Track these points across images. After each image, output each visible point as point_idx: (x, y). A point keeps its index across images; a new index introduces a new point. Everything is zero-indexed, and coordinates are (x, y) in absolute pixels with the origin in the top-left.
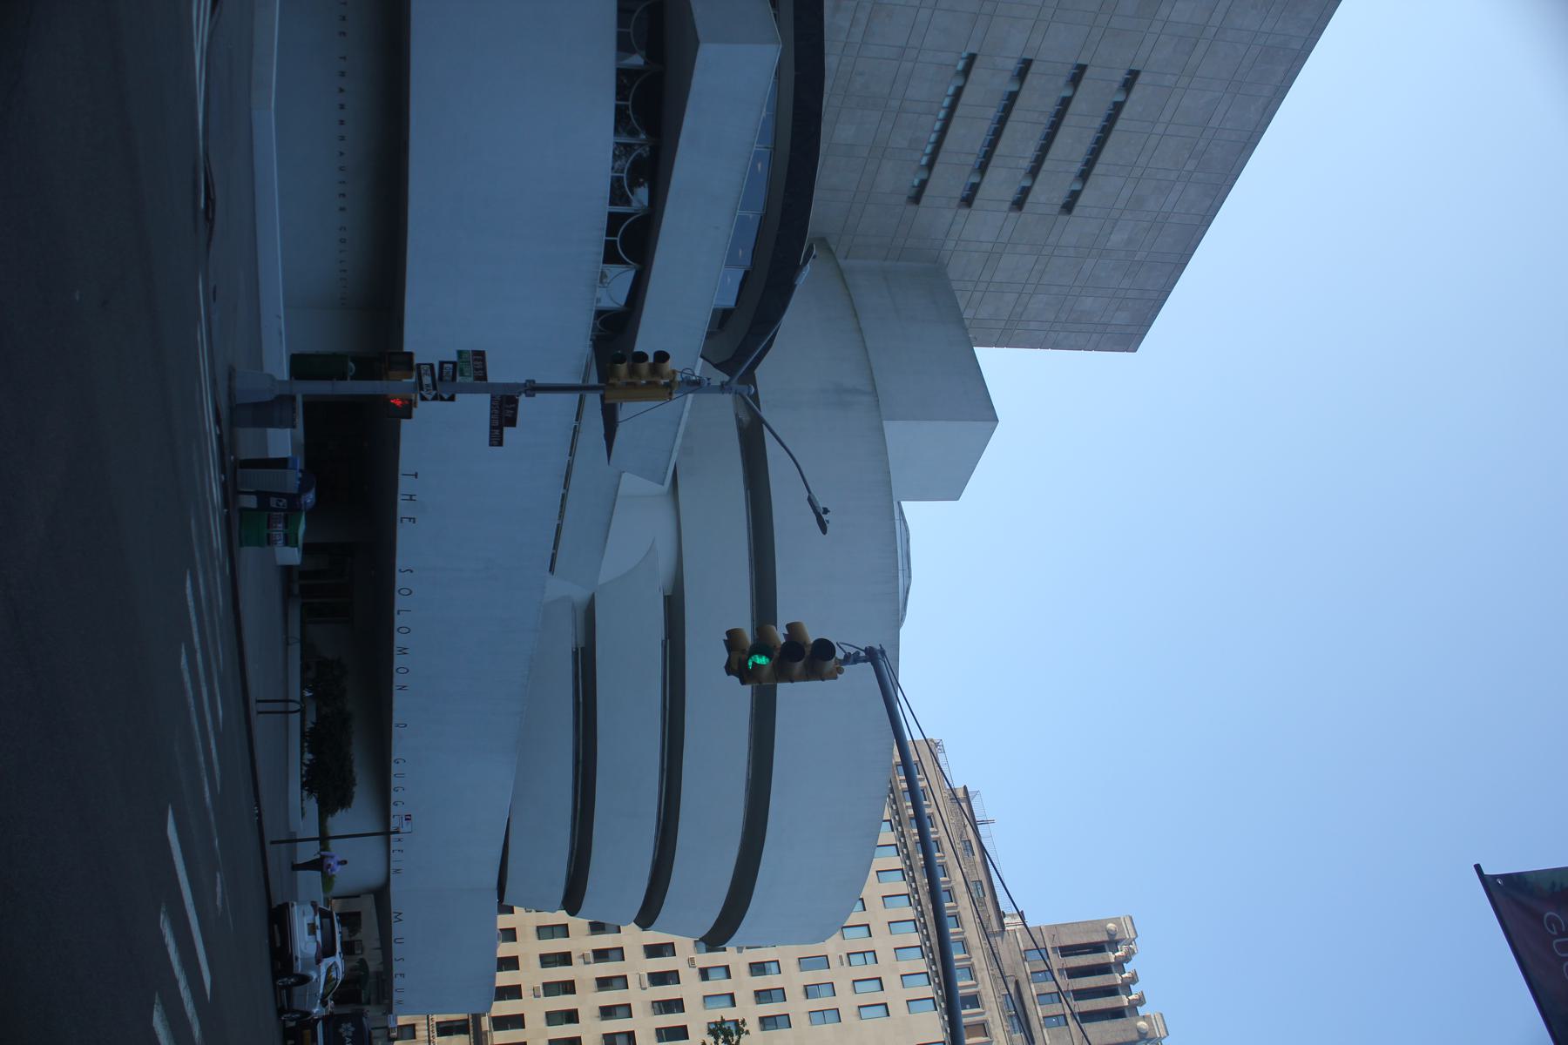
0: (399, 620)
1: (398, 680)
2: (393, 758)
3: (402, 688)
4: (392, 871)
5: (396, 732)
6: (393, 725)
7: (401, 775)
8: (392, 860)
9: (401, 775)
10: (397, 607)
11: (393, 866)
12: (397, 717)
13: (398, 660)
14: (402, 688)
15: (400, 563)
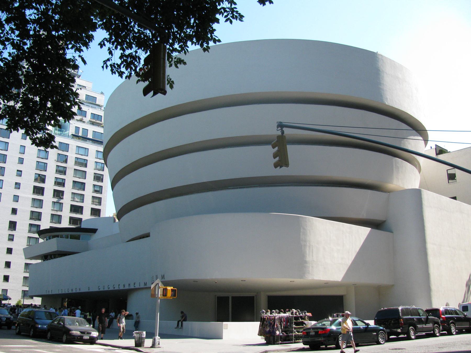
0: (67, 292)
1: (78, 291)
2: (98, 290)
3: (80, 289)
4: (146, 286)
5: (91, 290)
6: (89, 291)
7: (104, 287)
8: (139, 287)
9: (104, 287)
10: (64, 293)
11: (142, 286)
12: (86, 290)
13: (74, 291)
14: (80, 289)
15: (58, 293)
